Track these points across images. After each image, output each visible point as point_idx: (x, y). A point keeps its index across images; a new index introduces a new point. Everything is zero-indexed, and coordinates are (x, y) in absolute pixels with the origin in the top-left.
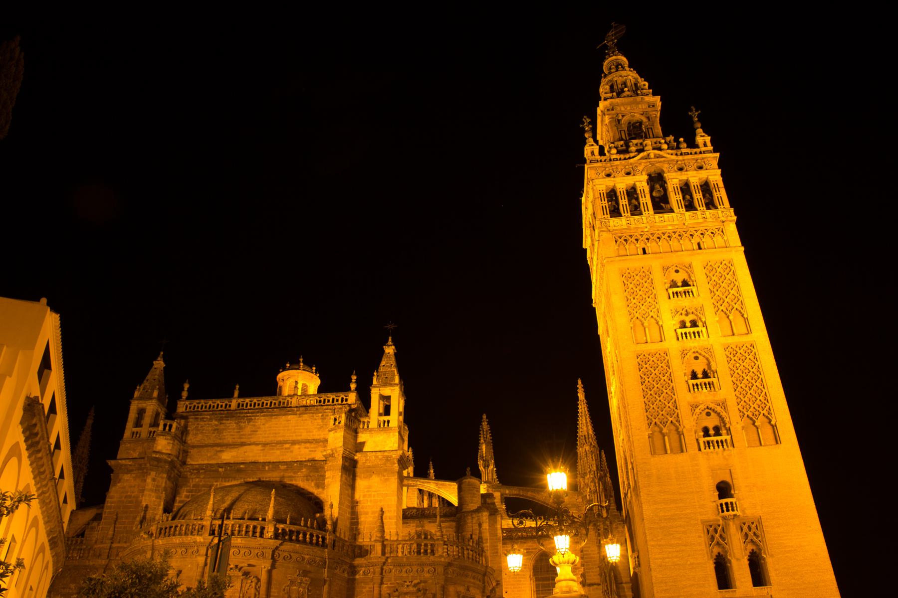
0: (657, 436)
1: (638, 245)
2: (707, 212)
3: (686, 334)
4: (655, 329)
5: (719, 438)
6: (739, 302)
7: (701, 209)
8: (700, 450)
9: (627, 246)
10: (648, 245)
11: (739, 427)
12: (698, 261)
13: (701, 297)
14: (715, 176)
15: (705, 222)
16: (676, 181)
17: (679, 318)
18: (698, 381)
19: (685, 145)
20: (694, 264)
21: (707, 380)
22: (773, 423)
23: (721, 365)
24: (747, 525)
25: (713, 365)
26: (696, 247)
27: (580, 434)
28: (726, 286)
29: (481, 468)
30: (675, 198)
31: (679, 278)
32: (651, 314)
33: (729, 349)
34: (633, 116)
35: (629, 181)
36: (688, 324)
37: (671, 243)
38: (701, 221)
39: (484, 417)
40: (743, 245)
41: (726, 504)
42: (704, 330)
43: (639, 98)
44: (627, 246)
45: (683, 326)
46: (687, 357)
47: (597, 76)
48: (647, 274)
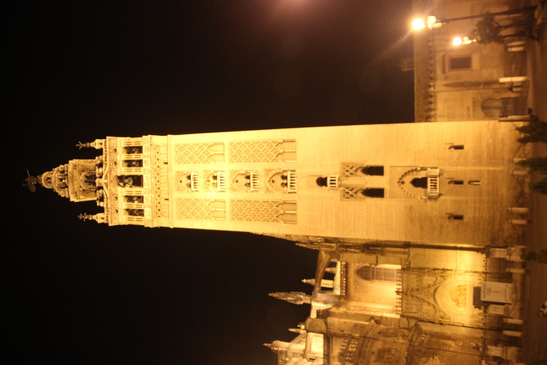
0: (285, 217)
1: (163, 203)
4: (217, 204)
5: (289, 178)
6: (203, 146)
7: (141, 157)
8: (295, 193)
9: (163, 210)
10: (163, 196)
11: (282, 164)
12: (176, 167)
13: (199, 170)
14: (121, 142)
16: (123, 169)
17: (211, 188)
19: (100, 157)
20: (177, 170)
22: (282, 141)
23: (244, 167)
24: (345, 172)
26: (166, 166)
29: (302, 303)
30: (134, 171)
31: (185, 181)
32: (207, 205)
33: (233, 159)
34: (81, 180)
37: (162, 182)
38: (149, 159)
39: (270, 295)
40: (166, 135)
43: (69, 175)
44: (163, 210)
45: (215, 185)
46: (236, 188)
48: (181, 202)
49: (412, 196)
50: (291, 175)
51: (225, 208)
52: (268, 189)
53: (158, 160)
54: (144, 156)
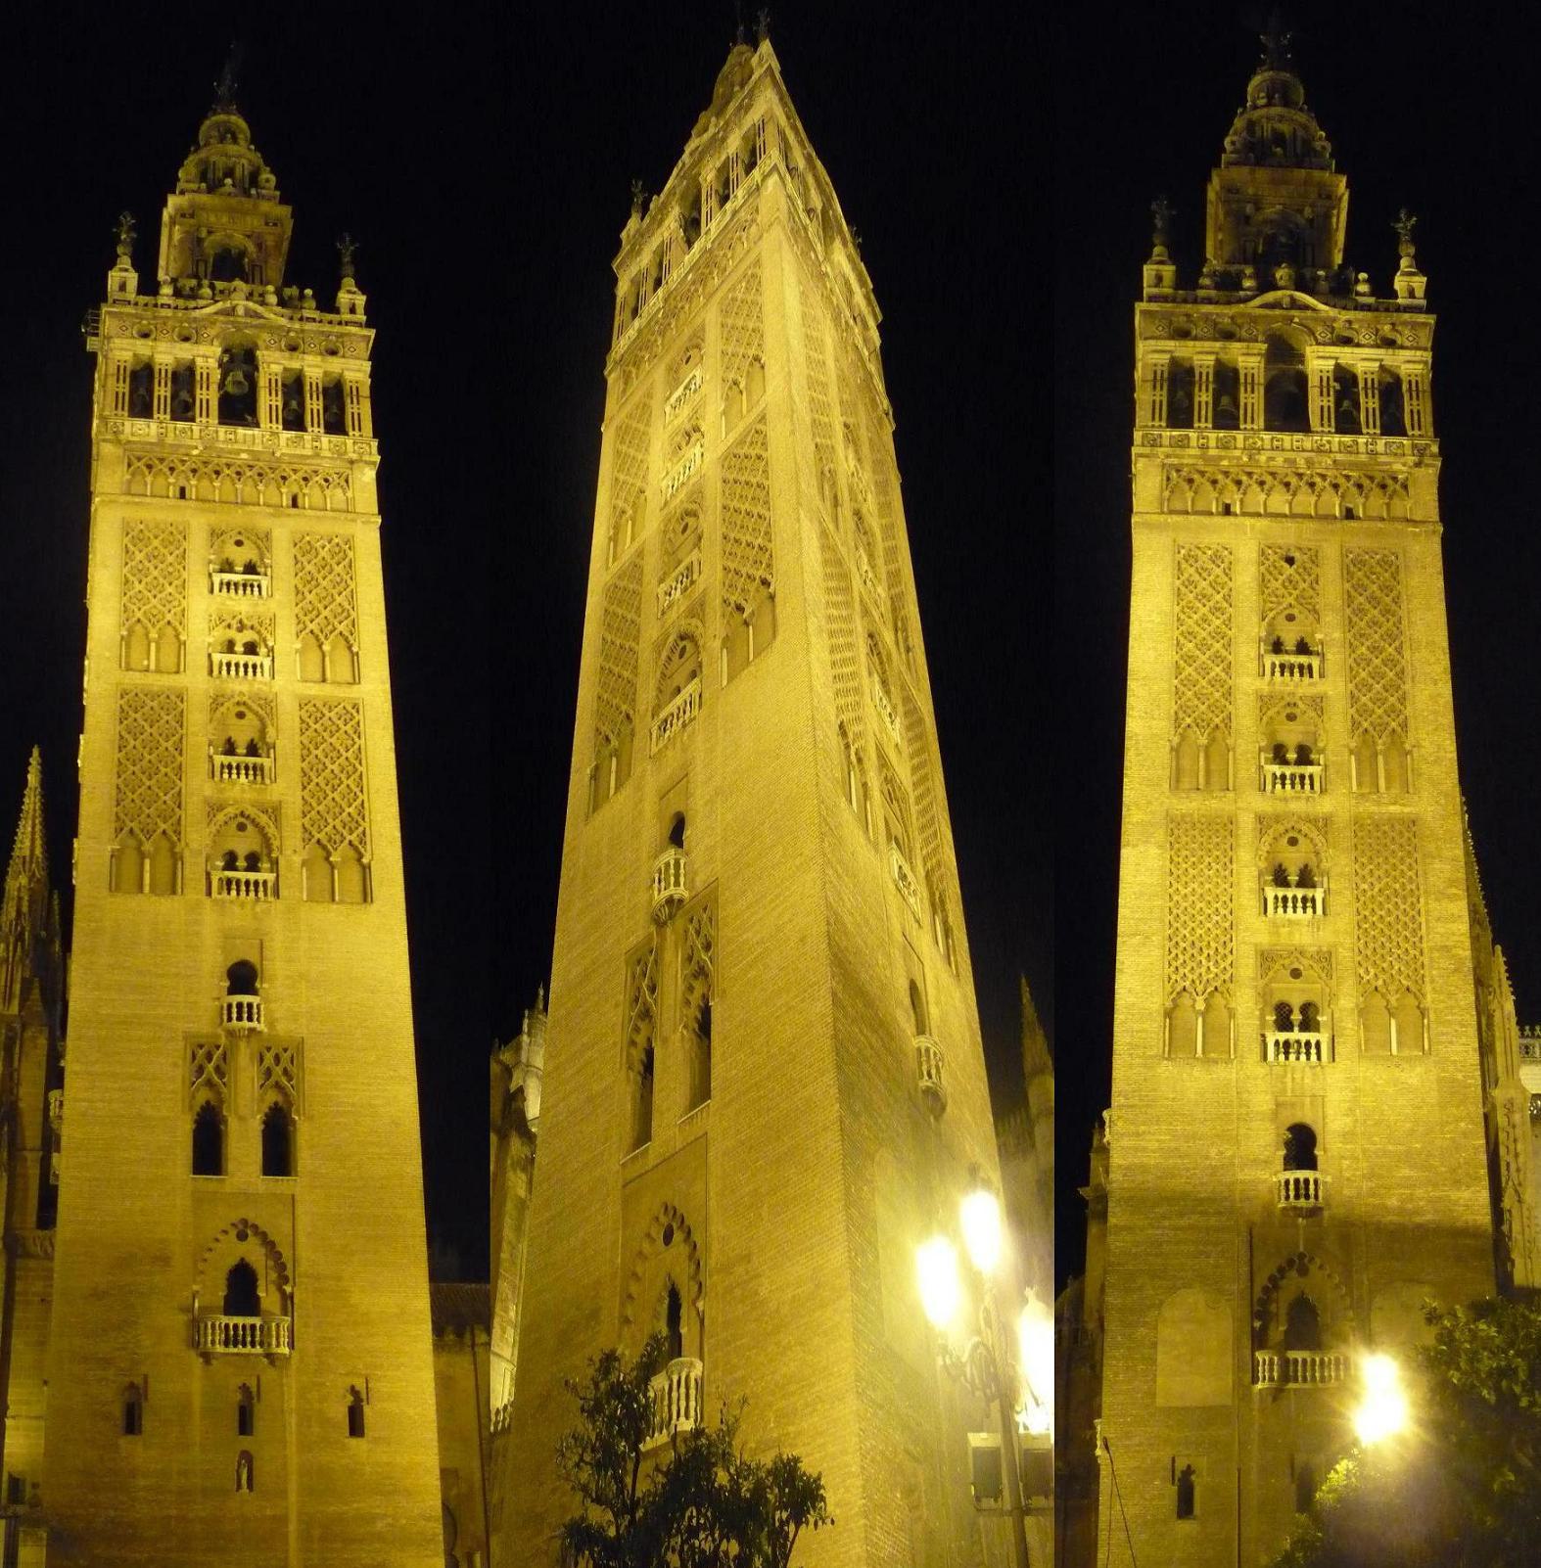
1: (172, 480)
2: (325, 439)
3: (229, 665)
5: (252, 876)
8: (209, 893)
10: (193, 482)
11: (297, 859)
12: (283, 531)
13: (276, 602)
15: (317, 455)
16: (276, 368)
17: (221, 634)
18: (233, 760)
21: (251, 760)
22: (365, 861)
23: (286, 737)
25: (271, 732)
26: (286, 501)
27: (16, 853)
28: (330, 588)
30: (268, 401)
31: (240, 556)
35: (185, 352)
36: (239, 648)
38: (310, 453)
40: (380, 512)
41: (240, 1006)
42: (267, 662)
47: (188, 141)
48: (175, 538)
49: (201, 1266)
50: (265, 882)
51: (158, 671)
52: (221, 808)
53: (305, 479)
54: (314, 441)
